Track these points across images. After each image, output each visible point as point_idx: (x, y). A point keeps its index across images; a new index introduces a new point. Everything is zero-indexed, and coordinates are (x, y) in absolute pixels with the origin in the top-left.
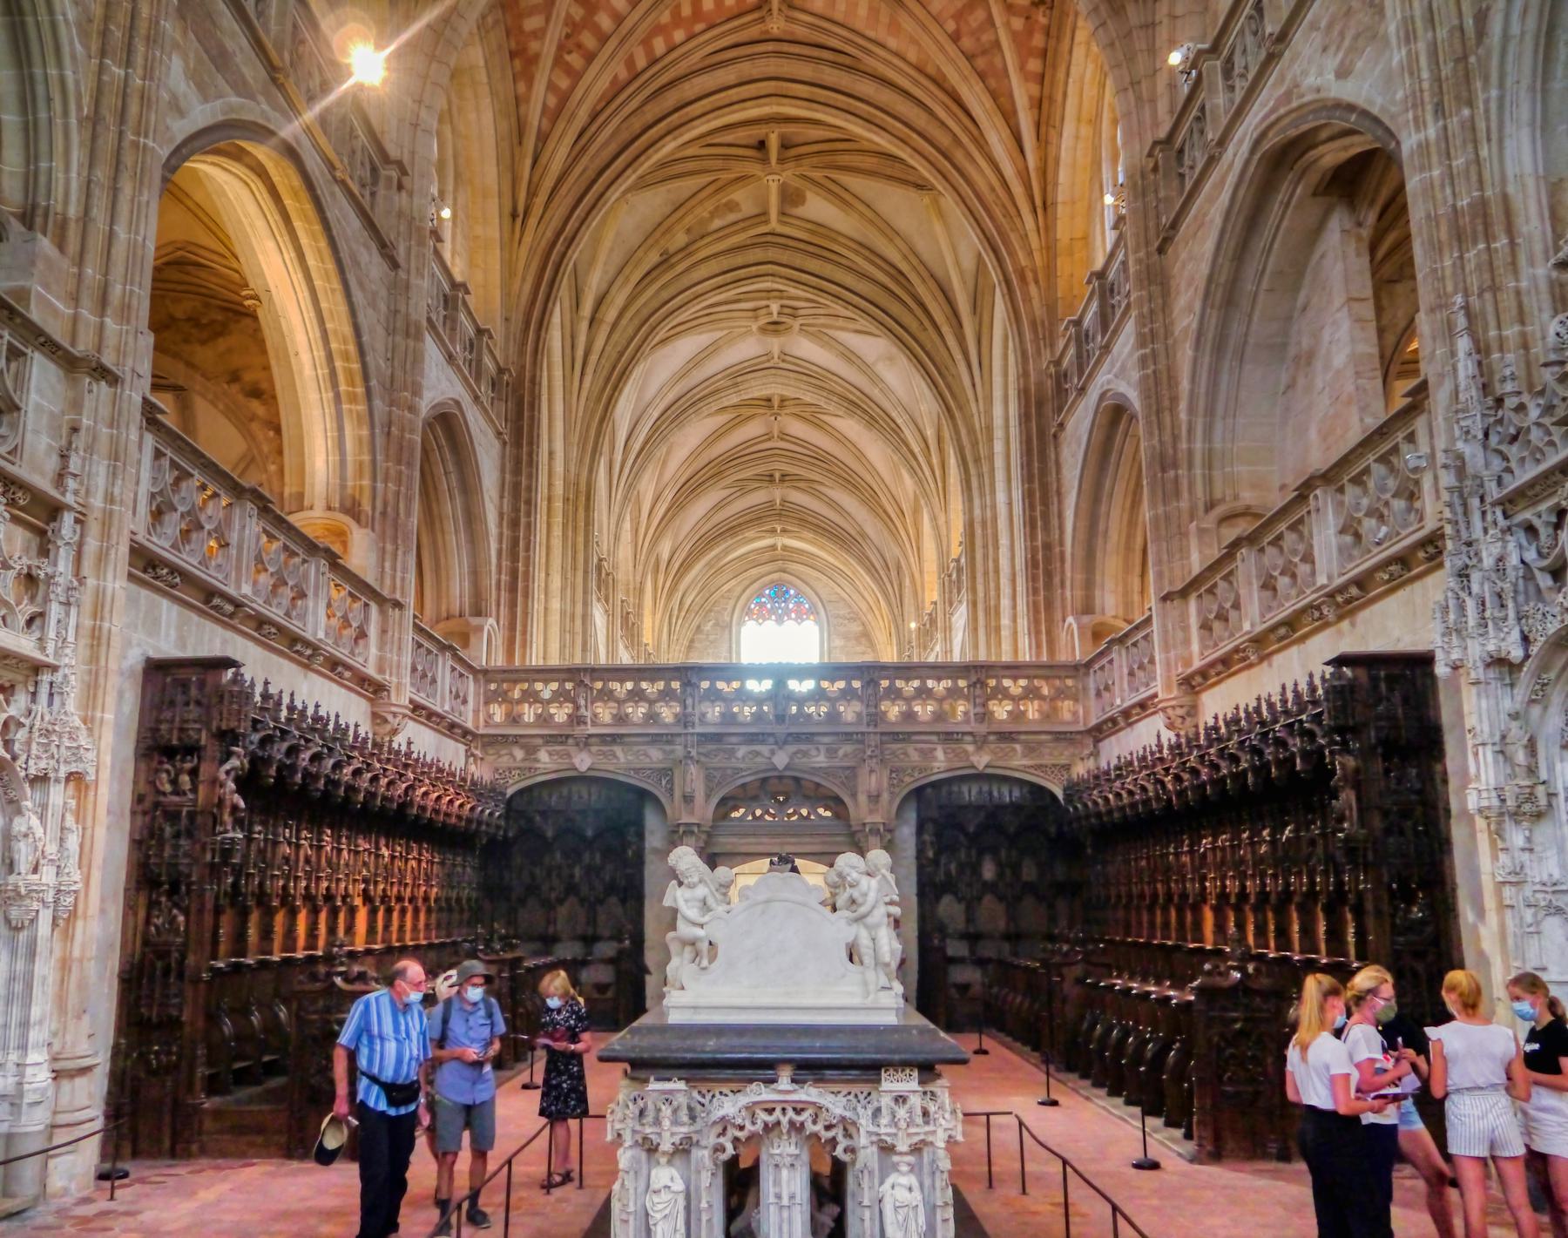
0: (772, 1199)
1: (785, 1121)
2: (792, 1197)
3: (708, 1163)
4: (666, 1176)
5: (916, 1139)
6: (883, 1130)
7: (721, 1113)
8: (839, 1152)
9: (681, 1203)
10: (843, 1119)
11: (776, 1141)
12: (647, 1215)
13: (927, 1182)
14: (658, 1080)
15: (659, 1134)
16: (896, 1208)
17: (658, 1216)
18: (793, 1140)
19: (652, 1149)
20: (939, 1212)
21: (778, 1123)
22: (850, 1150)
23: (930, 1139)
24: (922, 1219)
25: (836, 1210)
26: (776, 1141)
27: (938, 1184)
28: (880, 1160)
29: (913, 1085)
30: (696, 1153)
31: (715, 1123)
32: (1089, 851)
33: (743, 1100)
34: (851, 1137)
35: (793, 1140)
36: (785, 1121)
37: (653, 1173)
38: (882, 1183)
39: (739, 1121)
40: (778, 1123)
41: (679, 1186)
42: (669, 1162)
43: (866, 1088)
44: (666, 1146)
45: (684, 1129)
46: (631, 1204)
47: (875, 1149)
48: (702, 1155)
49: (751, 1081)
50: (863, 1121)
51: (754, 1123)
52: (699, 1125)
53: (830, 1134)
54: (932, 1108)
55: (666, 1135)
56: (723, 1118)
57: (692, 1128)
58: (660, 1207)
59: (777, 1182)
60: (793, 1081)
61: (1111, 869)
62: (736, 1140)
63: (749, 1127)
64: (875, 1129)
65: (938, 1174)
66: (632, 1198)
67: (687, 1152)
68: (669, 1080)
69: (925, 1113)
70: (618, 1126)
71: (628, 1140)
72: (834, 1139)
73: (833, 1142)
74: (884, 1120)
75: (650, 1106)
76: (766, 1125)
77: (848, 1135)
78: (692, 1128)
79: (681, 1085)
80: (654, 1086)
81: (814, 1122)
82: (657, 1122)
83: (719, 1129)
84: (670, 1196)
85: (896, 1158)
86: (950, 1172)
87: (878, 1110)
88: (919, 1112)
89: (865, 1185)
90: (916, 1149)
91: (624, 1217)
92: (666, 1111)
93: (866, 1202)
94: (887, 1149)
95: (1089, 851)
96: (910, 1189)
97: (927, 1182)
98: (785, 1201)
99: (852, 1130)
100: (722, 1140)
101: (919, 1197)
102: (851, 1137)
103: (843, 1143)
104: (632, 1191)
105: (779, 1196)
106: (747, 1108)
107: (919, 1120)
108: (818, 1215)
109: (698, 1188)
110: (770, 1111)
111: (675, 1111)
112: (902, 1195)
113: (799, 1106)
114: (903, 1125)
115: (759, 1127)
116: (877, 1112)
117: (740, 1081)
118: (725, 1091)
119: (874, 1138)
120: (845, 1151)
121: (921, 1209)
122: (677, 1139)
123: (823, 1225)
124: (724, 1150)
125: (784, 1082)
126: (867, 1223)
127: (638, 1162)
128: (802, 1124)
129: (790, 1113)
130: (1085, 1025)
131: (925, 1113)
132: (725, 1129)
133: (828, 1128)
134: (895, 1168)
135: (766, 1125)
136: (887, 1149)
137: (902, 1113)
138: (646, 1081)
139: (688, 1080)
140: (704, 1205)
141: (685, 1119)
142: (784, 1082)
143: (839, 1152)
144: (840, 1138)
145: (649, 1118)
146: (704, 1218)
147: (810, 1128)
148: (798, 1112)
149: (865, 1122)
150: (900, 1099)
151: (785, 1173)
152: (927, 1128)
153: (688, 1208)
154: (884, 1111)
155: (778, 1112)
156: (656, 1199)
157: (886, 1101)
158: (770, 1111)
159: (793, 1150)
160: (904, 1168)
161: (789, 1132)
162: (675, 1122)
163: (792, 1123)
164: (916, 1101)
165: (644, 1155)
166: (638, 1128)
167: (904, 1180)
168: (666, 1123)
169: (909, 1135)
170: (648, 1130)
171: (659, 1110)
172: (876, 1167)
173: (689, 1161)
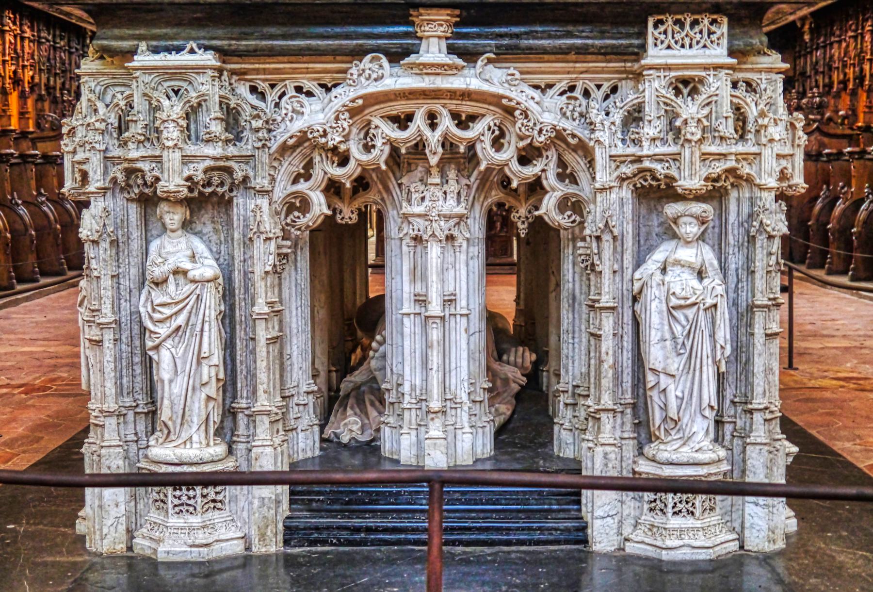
0: (408, 307)
1: (433, 138)
2: (449, 301)
3: (269, 225)
4: (181, 250)
5: (719, 168)
6: (647, 149)
7: (298, 125)
8: (548, 207)
9: (212, 303)
10: (560, 136)
11: (416, 187)
12: (143, 329)
13: (735, 261)
14: (156, 51)
15: (157, 159)
16: (671, 310)
17: (163, 330)
18: (452, 187)
19: (148, 201)
20: (759, 317)
21: (419, 148)
22: (573, 205)
23: (746, 169)
24: (723, 333)
25: (530, 357)
26: (416, 187)
27: (760, 262)
28: (637, 218)
29: (719, 54)
30: (244, 205)
31: (285, 149)
32: (807, 37)
33: (344, 95)
34: (574, 181)
35: (452, 187)
36: (433, 138)
37: (154, 246)
38: (638, 263)
39: (334, 139)
40: (419, 148)
41: (208, 268)
42: (186, 225)
43: (606, 71)
44: (173, 182)
45: (216, 150)
46: (107, 309)
47: (626, 193)
48: (256, 211)
49: (359, 53)
50: (603, 136)
51: (368, 148)
52: (246, 148)
53: (530, 171)
54: (752, 112)
55: (173, 158)
56: (303, 138)
57: (231, 150)
58: (167, 311)
59: (418, 273)
60: (452, 50)
61: (835, 51)
62: (333, 188)
63: (356, 152)
64: (632, 150)
65: (761, 240)
66: (108, 295)
67: (225, 203)
68: (179, 50)
69: (740, 117)
70: (79, 157)
71: (96, 182)
73: (536, 188)
74: (649, 131)
75: (139, 103)
77: (566, 175)
78: (231, 150)
79: (209, 59)
80: (144, 58)
81: (497, 144)
82: (153, 134)
83: (293, 164)
84: (188, 288)
85: (672, 209)
86: (784, 238)
87: (639, 108)
88: (726, 109)
89: (606, 266)
90: (715, 194)
91: (93, 333)
92: (173, 109)
93: (606, 300)
94: (654, 192)
95: (807, 37)
96: (701, 275)
97: (735, 261)
98: (435, 308)
99: (576, 162)
100: (302, 186)
101: (720, 290)
102: (574, 181)
103: (556, 190)
104: (106, 282)
105: (421, 300)
106: (354, 112)
107: (728, 128)
108: (496, 366)
109: (247, 275)
110: (403, 121)
111: (192, 112)
112: (682, 283)
113: (467, 108)
114: (693, 132)
115: (380, 154)
116: (634, 117)
117: (334, 53)
118: (308, 85)
119: (628, 170)
120: (563, 204)
121: (723, 315)
122: (197, 170)
123: (506, 381)
124: (305, 205)
125: (433, 51)
126: (607, 344)
127: (124, 223)
128: (471, 147)
129: (446, 123)
130: (819, 205)
131: (740, 117)
132: (309, 165)
133: (524, 160)
134: (670, 233)
135: (395, 151)
136: (654, 192)
137: (689, 109)
138: (132, 53)
139: (223, 53)
140: (261, 307)
141: (217, 128)
142: (433, 51)
143: (548, 207)
144: (550, 179)
145: (136, 129)
146: (263, 333)
147: (487, 155)
148: (463, 121)
149: (607, 140)
150: (686, 85)
151: (434, 251)
152: (740, 148)
153: (228, 319)
154: (651, 111)
155: (419, 122)
156: (158, 297)
157: (655, 88)
159: (451, 206)
160: (690, 229)
161: (442, 165)
162: (188, 134)
163: (447, 143)
164: (719, 86)
165: (134, 211)
166: (116, 152)
167: (687, 254)
168: (171, 134)
169: (705, 157)
170: (134, 154)
171: (158, 108)
172: (629, 229)
173: (229, 223)
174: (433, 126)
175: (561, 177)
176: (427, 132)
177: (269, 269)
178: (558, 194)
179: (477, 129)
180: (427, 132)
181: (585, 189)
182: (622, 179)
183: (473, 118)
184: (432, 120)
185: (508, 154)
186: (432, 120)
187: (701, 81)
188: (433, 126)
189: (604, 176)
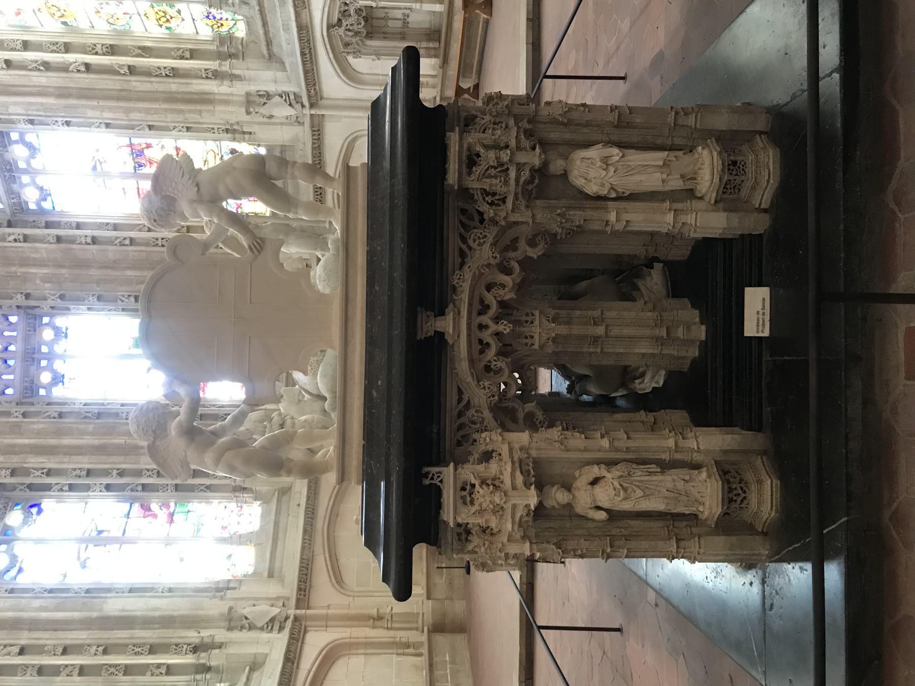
1: (493, 327)
36: (493, 327)
60: (442, 313)
67: (536, 462)
72: (518, 262)
73: (525, 263)
76: (500, 353)
82: (498, 510)
100: (521, 415)
102: (516, 239)
110: (484, 346)
113: (477, 306)
125: (446, 324)
129: (485, 319)
142: (446, 324)
144: (519, 255)
148: (484, 308)
150: (472, 160)
155: (486, 336)
158: (484, 346)
174: (487, 327)
175: (515, 249)
176: (490, 331)
177: (583, 436)
178: (528, 248)
179: (490, 298)
180: (490, 331)
181: (525, 231)
182: (527, 207)
183: (482, 301)
184: (482, 327)
185: (507, 280)
186: (482, 327)
187: (469, 149)
188: (487, 327)
189: (523, 216)
